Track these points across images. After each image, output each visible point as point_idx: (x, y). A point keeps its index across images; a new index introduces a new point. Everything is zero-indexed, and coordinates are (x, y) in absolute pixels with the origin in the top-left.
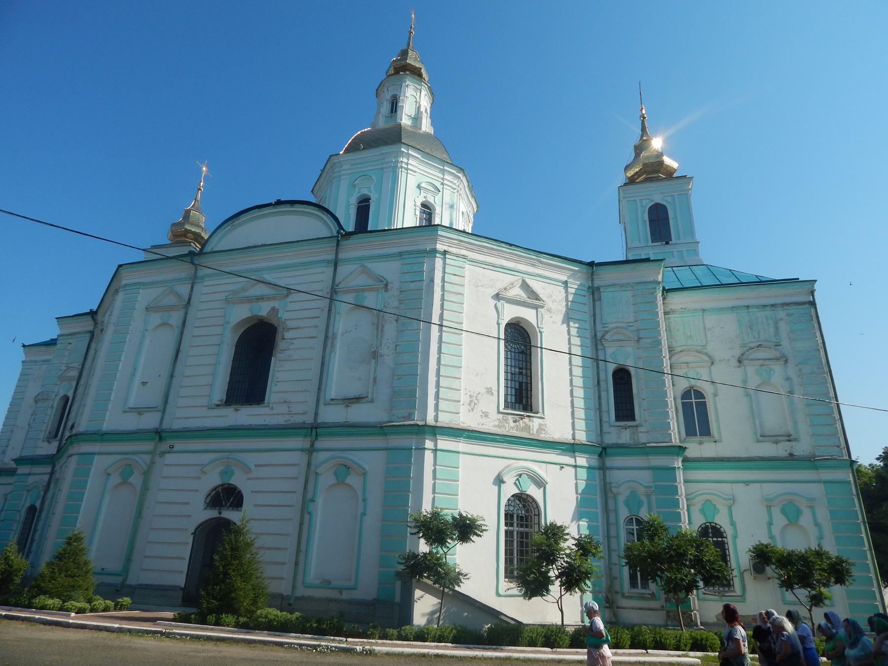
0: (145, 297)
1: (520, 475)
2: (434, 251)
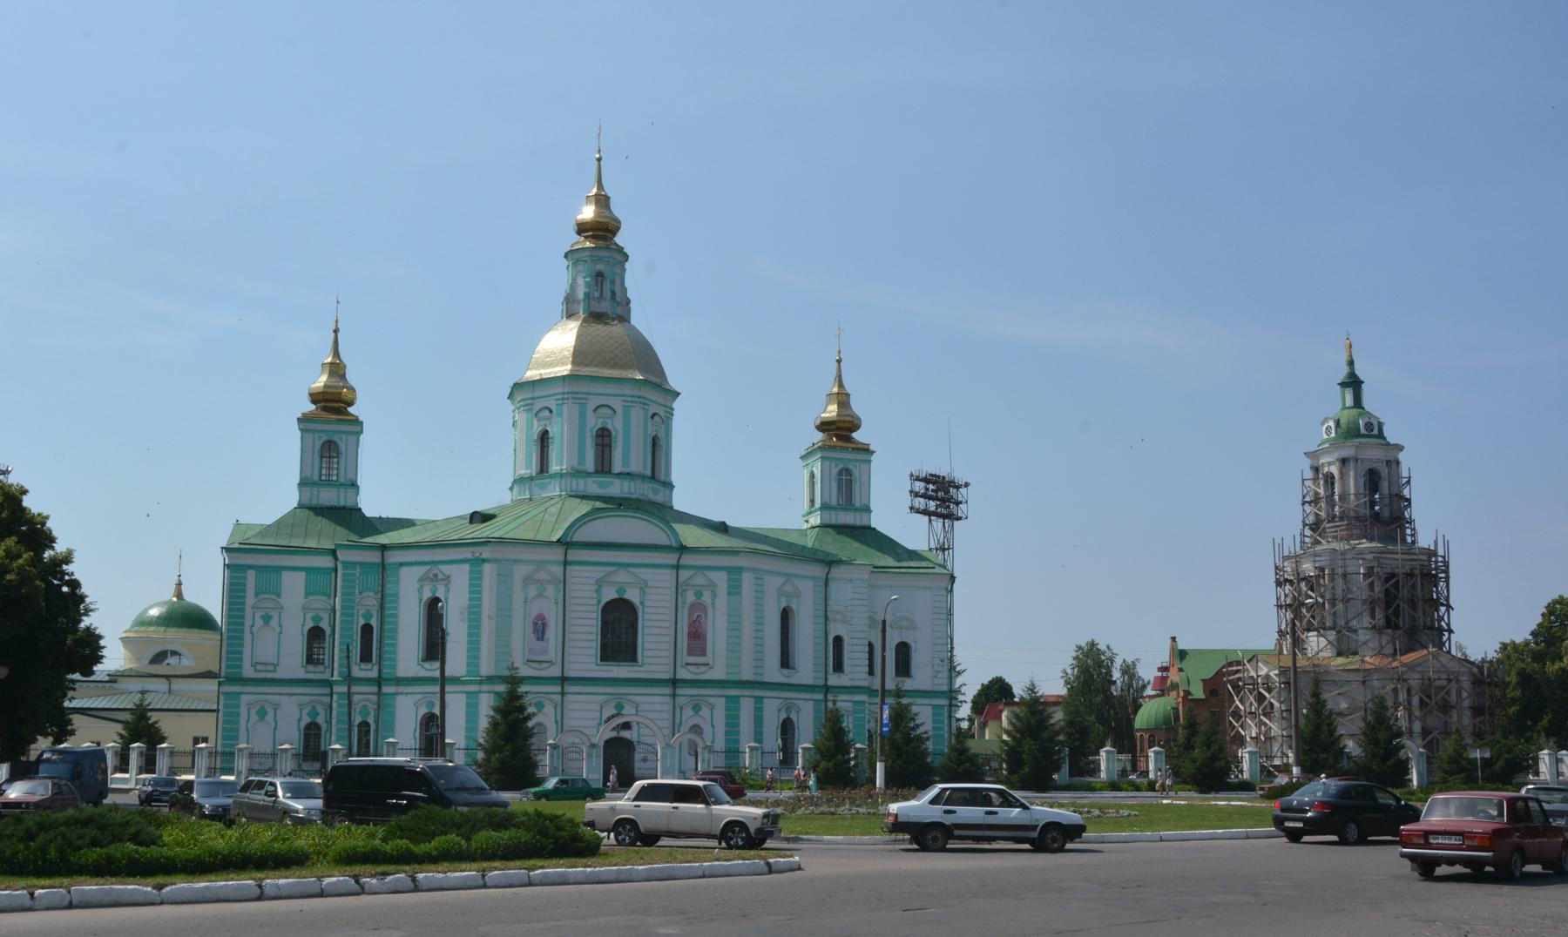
0: (520, 571)
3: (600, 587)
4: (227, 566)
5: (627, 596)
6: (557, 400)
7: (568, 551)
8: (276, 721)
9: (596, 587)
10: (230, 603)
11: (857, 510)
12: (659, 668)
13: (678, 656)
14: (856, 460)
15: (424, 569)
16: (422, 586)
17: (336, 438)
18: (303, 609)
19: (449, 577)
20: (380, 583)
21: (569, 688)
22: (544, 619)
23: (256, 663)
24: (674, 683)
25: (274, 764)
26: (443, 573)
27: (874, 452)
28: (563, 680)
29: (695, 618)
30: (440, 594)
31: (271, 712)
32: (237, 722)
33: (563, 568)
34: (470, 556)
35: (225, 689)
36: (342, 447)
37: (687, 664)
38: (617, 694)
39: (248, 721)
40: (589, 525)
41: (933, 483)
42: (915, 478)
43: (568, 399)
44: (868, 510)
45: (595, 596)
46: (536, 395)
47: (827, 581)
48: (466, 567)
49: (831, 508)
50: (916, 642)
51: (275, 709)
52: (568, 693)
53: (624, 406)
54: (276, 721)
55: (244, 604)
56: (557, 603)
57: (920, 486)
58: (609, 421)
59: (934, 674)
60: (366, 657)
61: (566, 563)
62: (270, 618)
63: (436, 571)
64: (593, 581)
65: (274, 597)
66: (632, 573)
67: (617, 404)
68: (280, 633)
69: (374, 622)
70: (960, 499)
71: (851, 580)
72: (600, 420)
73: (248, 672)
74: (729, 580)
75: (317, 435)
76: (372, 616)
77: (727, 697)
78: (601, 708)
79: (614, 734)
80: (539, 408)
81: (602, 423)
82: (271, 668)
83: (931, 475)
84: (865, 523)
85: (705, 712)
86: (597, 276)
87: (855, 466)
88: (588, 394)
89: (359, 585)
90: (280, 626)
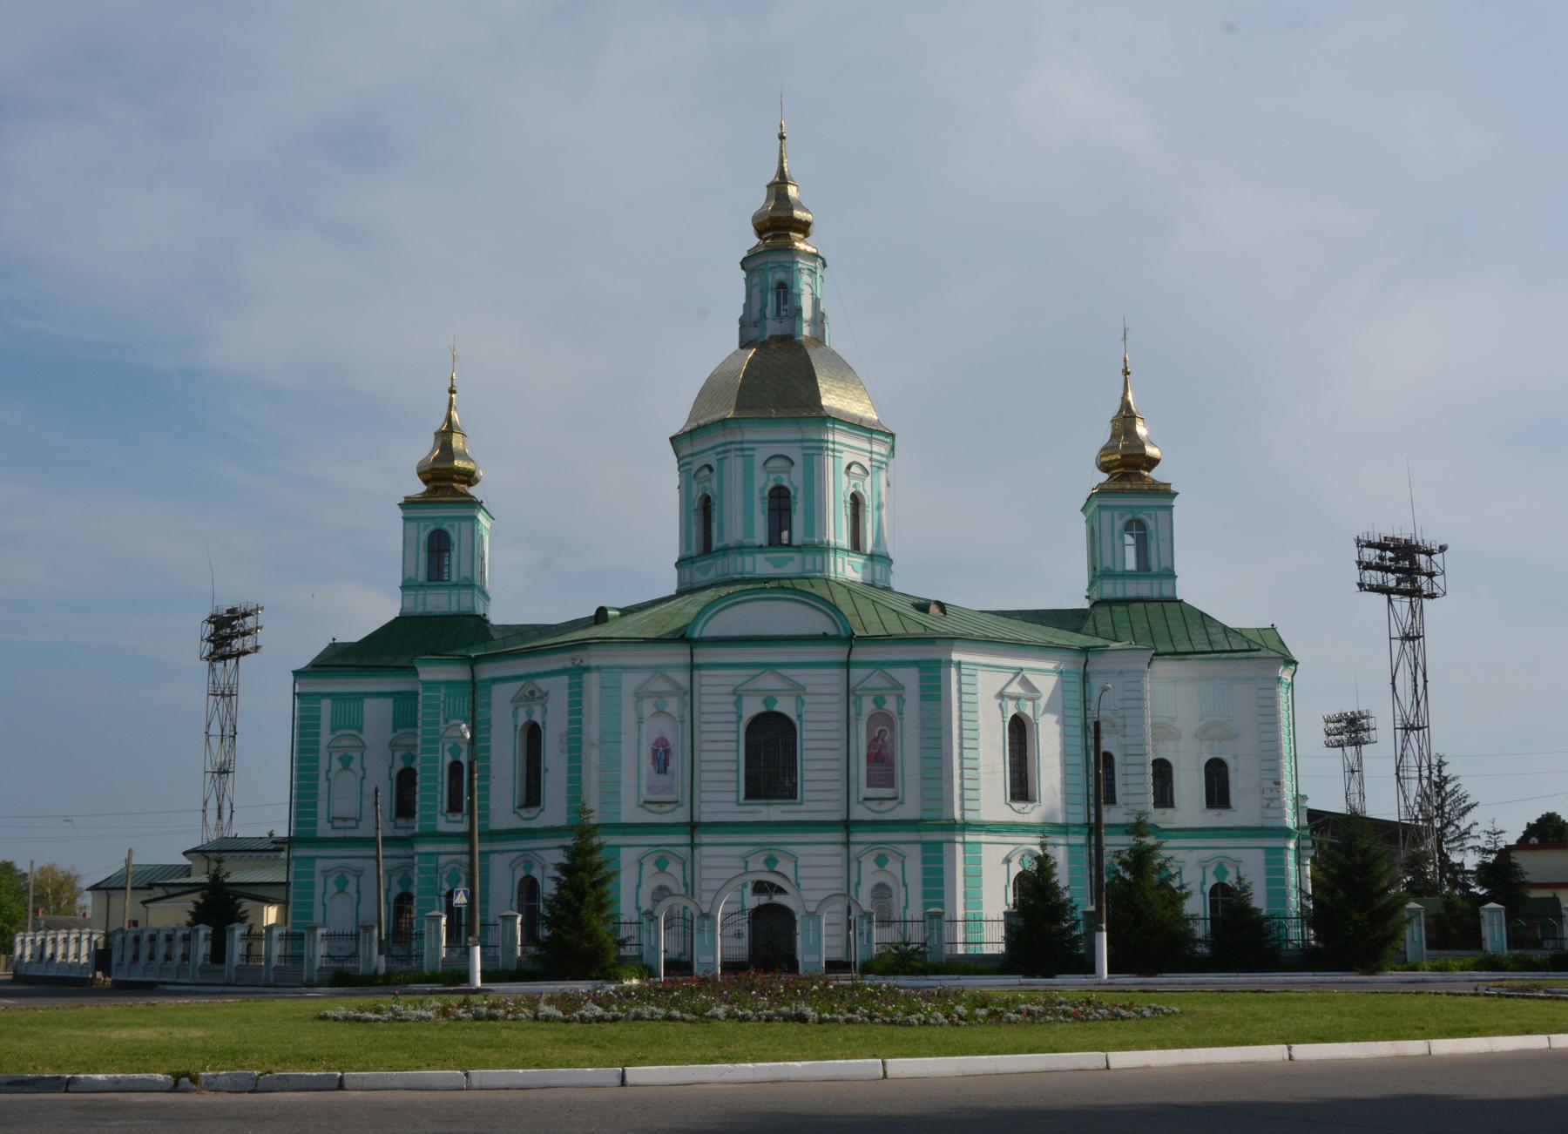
0: (630, 682)
1: (1023, 856)
2: (950, 662)
3: (740, 696)
4: (297, 695)
5: (776, 708)
6: (717, 454)
7: (695, 651)
8: (358, 892)
9: (734, 698)
10: (300, 743)
11: (1159, 576)
12: (823, 806)
13: (853, 788)
14: (1148, 507)
15: (514, 687)
16: (516, 708)
17: (445, 526)
18: (390, 745)
19: (547, 694)
20: (471, 707)
21: (705, 839)
22: (667, 744)
23: (333, 818)
24: (848, 825)
25: (357, 947)
26: (540, 690)
27: (1176, 494)
28: (693, 827)
29: (877, 735)
30: (537, 718)
31: (352, 880)
32: (312, 896)
33: (689, 674)
34: (569, 664)
35: (299, 852)
36: (454, 536)
37: (865, 799)
38: (766, 844)
39: (324, 894)
40: (721, 614)
41: (1392, 550)
42: (1363, 544)
44: (1171, 575)
45: (735, 710)
46: (696, 449)
47: (1085, 677)
48: (564, 680)
49: (1117, 575)
50: (1235, 757)
51: (358, 877)
52: (701, 845)
53: (804, 455)
54: (358, 892)
55: (317, 743)
56: (682, 722)
57: (1371, 555)
58: (784, 477)
59: (1266, 803)
60: (455, 806)
61: (693, 667)
62: (351, 758)
63: (532, 688)
64: (730, 689)
65: (355, 732)
66: (785, 677)
67: (794, 453)
68: (363, 778)
69: (464, 759)
70: (1434, 569)
71: (1121, 672)
72: (772, 477)
73: (324, 830)
74: (922, 679)
75: (422, 524)
76: (460, 750)
77: (924, 843)
78: (746, 862)
79: (764, 900)
80: (698, 468)
81: (775, 480)
82: (353, 824)
83: (1386, 538)
84: (1166, 593)
85: (893, 866)
86: (777, 288)
87: (1150, 516)
89: (444, 711)
90: (363, 769)
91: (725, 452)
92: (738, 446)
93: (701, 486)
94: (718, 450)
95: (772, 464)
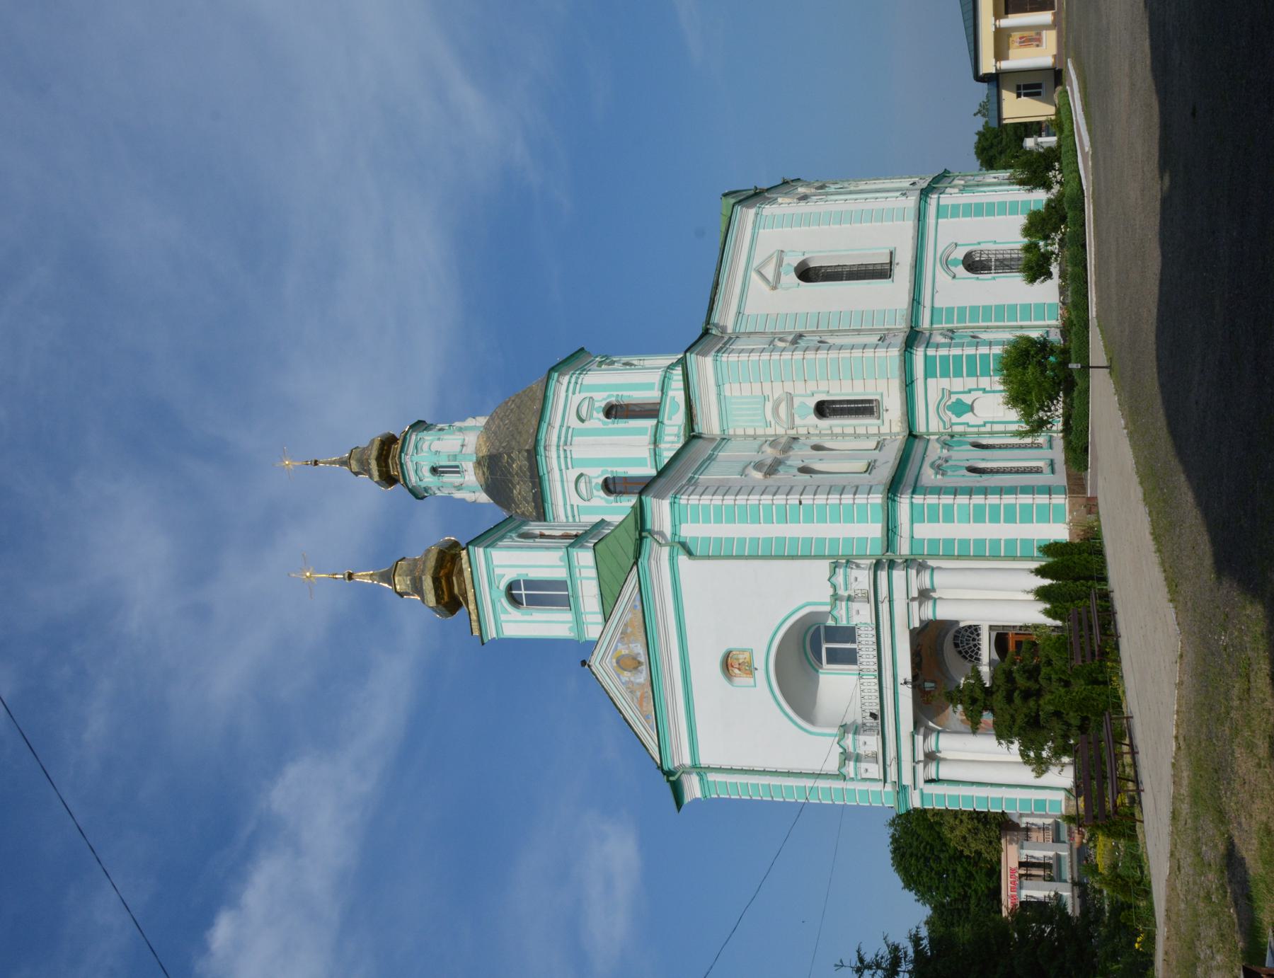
43: (565, 450)
58: (597, 405)
88: (562, 426)
91: (566, 457)
92: (562, 442)
93: (595, 492)
94: (563, 467)
95: (584, 414)
